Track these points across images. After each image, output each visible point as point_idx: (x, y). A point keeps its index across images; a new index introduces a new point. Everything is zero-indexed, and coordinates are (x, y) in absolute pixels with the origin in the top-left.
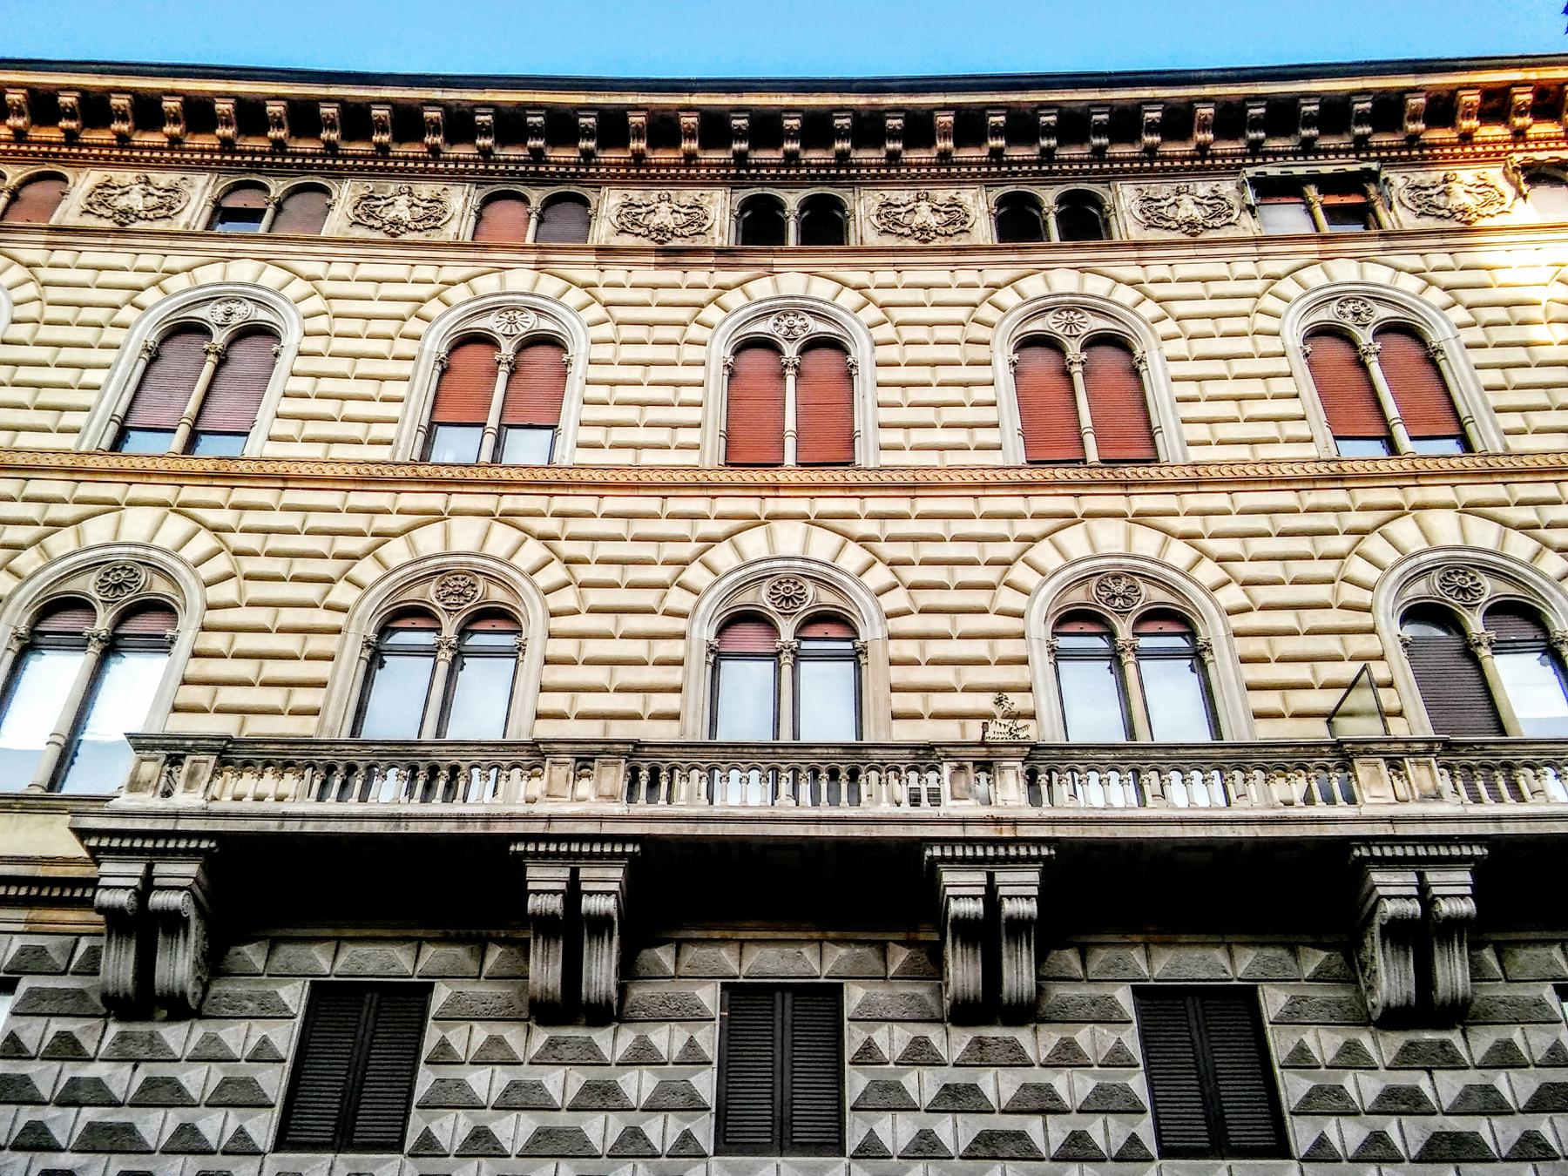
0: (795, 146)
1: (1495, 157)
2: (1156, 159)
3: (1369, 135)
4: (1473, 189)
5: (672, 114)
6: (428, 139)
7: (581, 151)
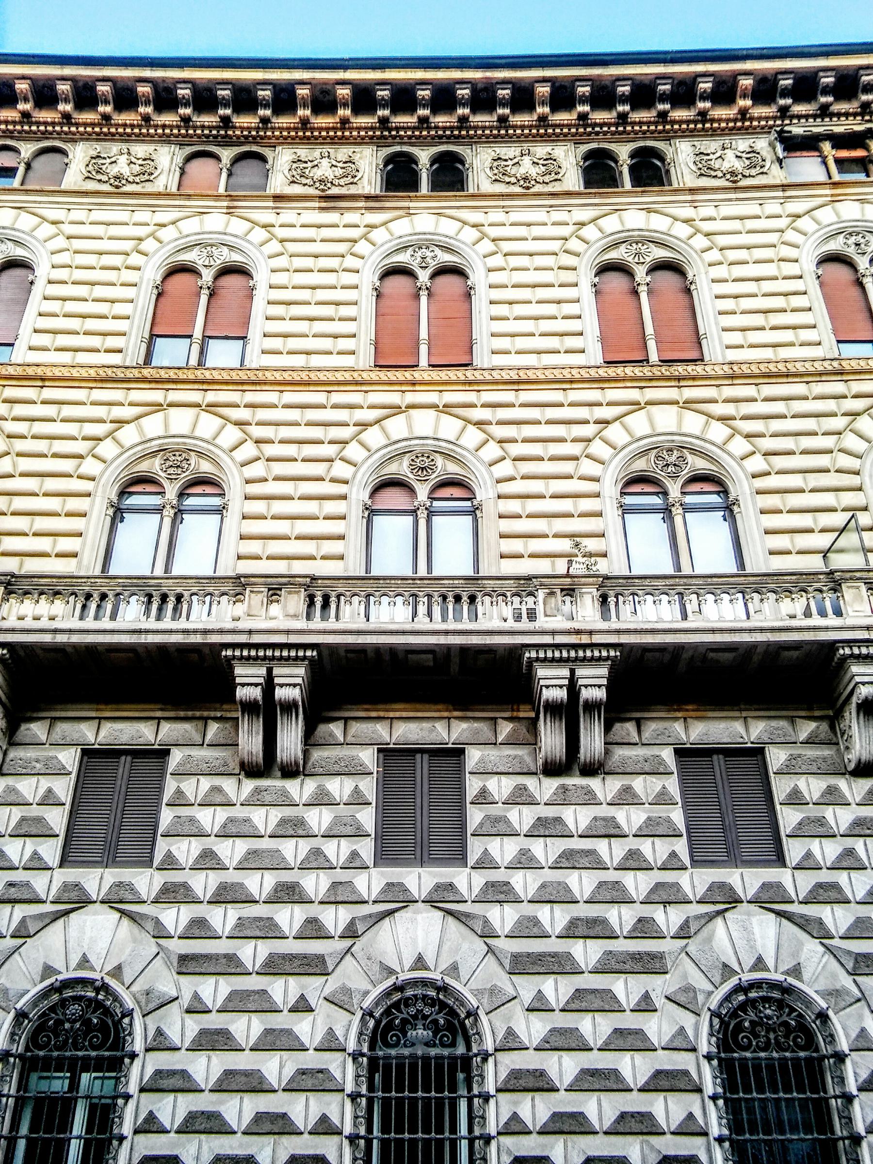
0: (387, 112)
1: (765, 130)
2: (588, 125)
3: (831, 104)
4: (744, 155)
5: (290, 87)
6: (101, 109)
7: (220, 117)
